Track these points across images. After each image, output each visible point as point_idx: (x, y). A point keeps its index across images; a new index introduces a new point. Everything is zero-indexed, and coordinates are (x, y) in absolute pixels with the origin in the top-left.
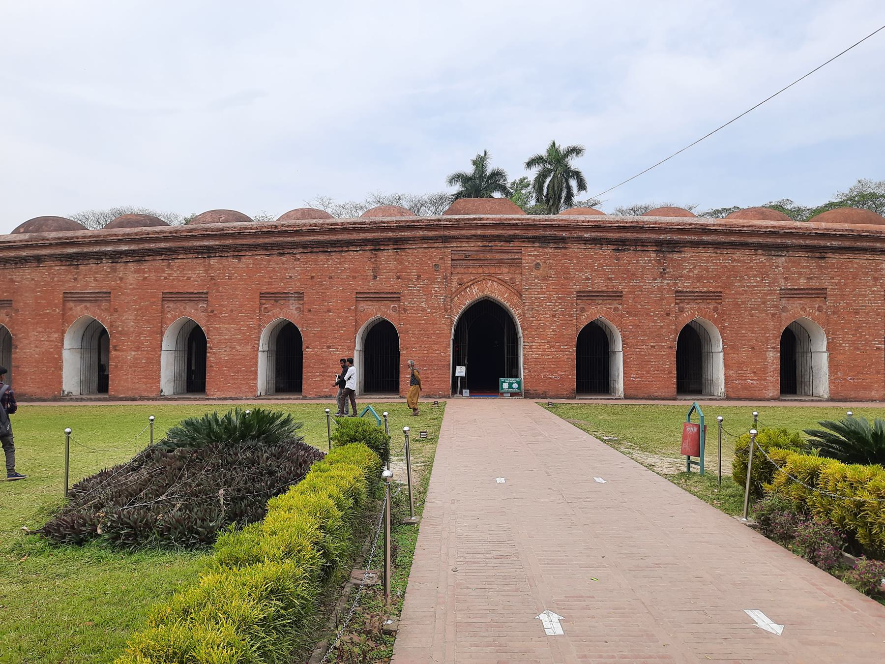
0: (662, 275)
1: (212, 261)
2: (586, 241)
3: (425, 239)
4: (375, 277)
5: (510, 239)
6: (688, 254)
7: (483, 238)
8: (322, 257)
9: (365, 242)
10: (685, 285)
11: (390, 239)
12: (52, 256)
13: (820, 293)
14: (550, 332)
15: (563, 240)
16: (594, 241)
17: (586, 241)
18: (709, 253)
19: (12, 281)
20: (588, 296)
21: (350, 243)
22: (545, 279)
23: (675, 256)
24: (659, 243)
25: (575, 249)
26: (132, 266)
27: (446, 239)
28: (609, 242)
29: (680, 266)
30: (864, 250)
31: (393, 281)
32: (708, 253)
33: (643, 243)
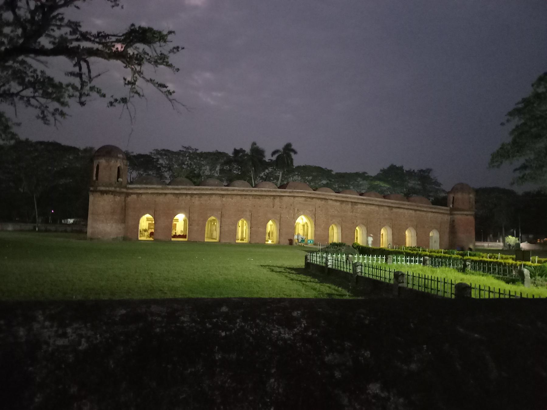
0: (352, 212)
1: (224, 199)
8: (257, 200)
9: (271, 196)
11: (278, 196)
12: (171, 193)
14: (322, 226)
16: (336, 201)
19: (155, 201)
21: (267, 196)
22: (321, 211)
25: (330, 202)
26: (197, 199)
27: (294, 197)
28: (339, 201)
31: (279, 208)
32: (364, 206)
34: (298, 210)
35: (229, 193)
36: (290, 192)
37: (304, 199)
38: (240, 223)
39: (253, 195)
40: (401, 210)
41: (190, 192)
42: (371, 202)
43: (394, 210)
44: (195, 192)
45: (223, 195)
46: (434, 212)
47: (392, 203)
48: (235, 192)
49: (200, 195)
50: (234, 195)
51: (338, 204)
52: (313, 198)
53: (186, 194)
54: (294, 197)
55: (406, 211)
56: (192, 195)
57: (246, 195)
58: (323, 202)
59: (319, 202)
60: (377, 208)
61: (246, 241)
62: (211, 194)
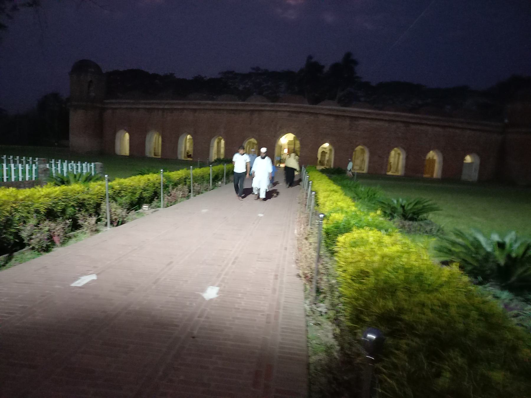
4: (250, 124)
7: (289, 111)
15: (316, 114)
23: (357, 123)
25: (322, 117)
32: (368, 122)
34: (280, 127)
35: (202, 107)
36: (271, 106)
37: (287, 114)
38: (393, 153)
39: (227, 110)
40: (424, 128)
41: (161, 107)
42: (378, 117)
43: (413, 127)
44: (166, 107)
45: (195, 110)
46: (473, 130)
47: (411, 118)
48: (208, 107)
49: (172, 110)
50: (207, 109)
51: (332, 119)
52: (299, 113)
53: (158, 109)
55: (430, 129)
56: (163, 110)
57: (220, 110)
58: (312, 118)
59: (307, 117)
60: (387, 125)
61: (401, 173)
62: (183, 109)
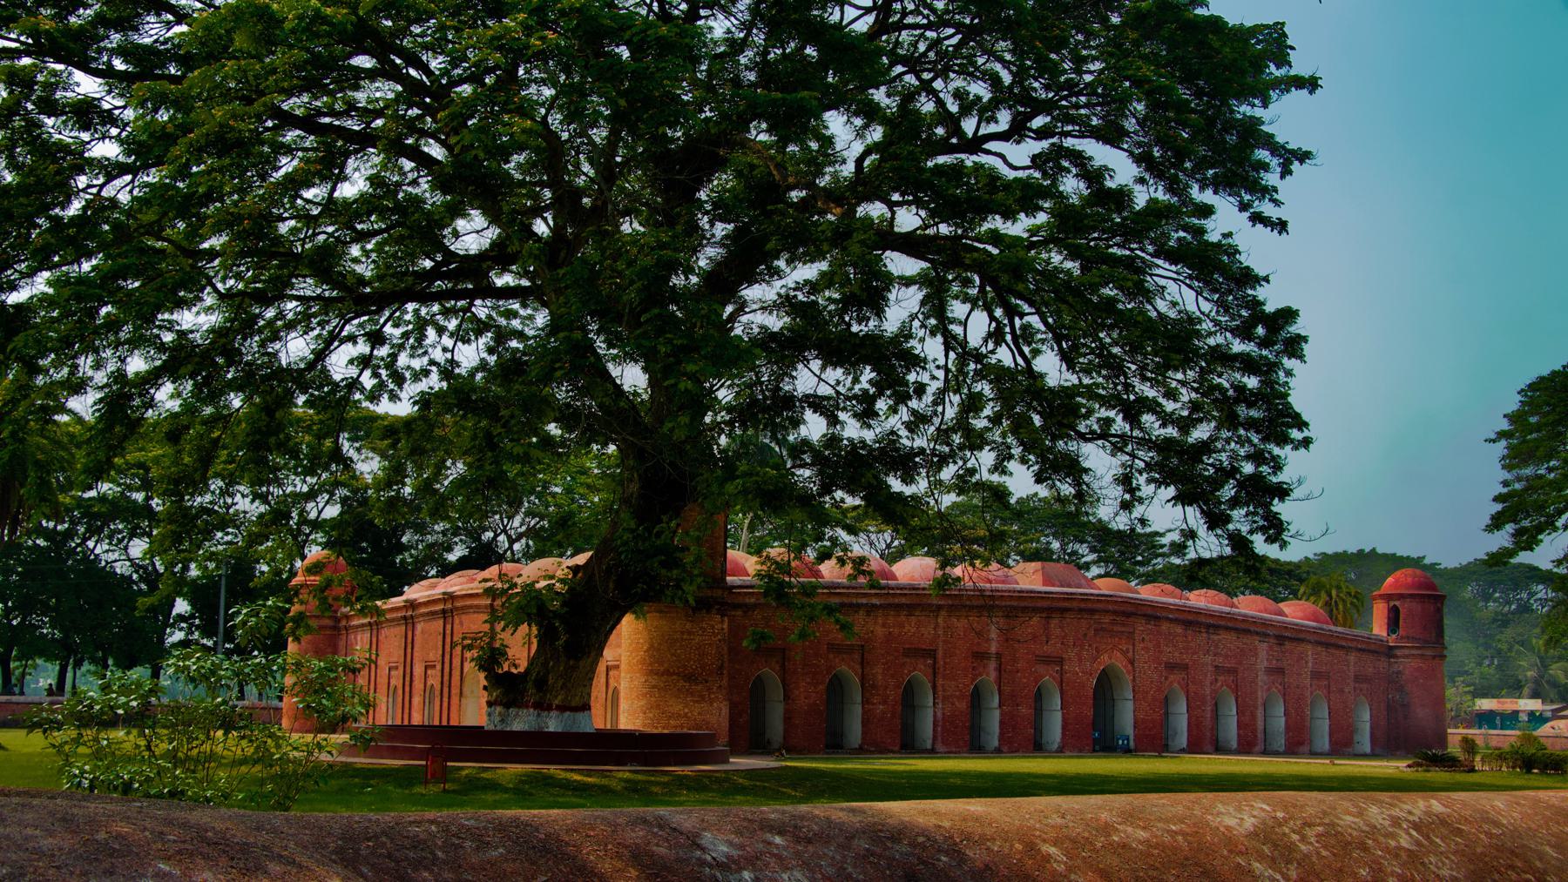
2: (1171, 620)
3: (1081, 610)
5: (1128, 615)
6: (1224, 636)
7: (1115, 613)
10: (1220, 661)
13: (1280, 671)
15: (1157, 618)
16: (1176, 621)
17: (1171, 620)
18: (1232, 636)
20: (1171, 667)
24: (1209, 626)
25: (1165, 626)
29: (1216, 647)
30: (1302, 640)
33: (1199, 624)
51: (1179, 630)
54: (1092, 611)
